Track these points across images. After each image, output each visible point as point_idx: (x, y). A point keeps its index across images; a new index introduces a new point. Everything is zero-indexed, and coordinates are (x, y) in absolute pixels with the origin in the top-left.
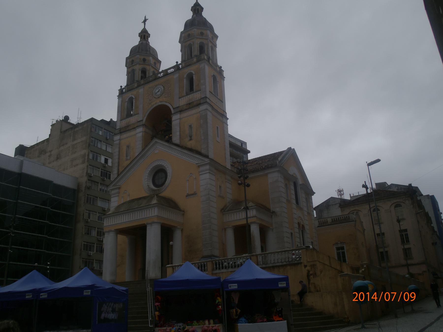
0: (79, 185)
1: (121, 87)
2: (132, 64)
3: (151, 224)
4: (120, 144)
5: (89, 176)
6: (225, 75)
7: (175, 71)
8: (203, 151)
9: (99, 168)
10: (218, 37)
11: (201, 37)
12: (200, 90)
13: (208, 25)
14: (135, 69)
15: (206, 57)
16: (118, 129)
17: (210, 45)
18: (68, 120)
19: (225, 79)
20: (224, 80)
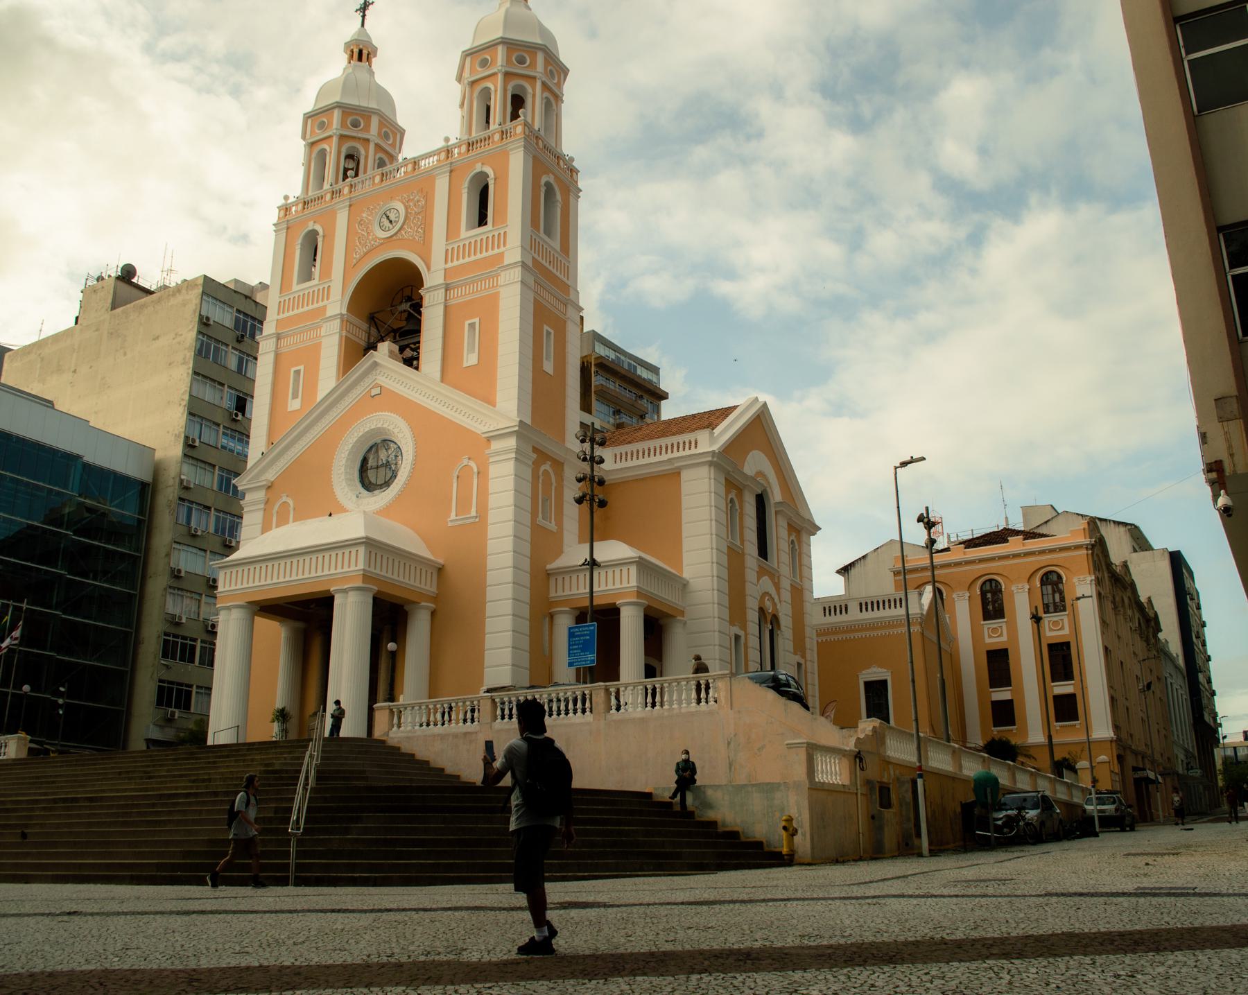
0: (157, 470)
1: (286, 198)
3: (345, 591)
9: (218, 425)
10: (568, 70)
18: (133, 278)
19: (580, 194)
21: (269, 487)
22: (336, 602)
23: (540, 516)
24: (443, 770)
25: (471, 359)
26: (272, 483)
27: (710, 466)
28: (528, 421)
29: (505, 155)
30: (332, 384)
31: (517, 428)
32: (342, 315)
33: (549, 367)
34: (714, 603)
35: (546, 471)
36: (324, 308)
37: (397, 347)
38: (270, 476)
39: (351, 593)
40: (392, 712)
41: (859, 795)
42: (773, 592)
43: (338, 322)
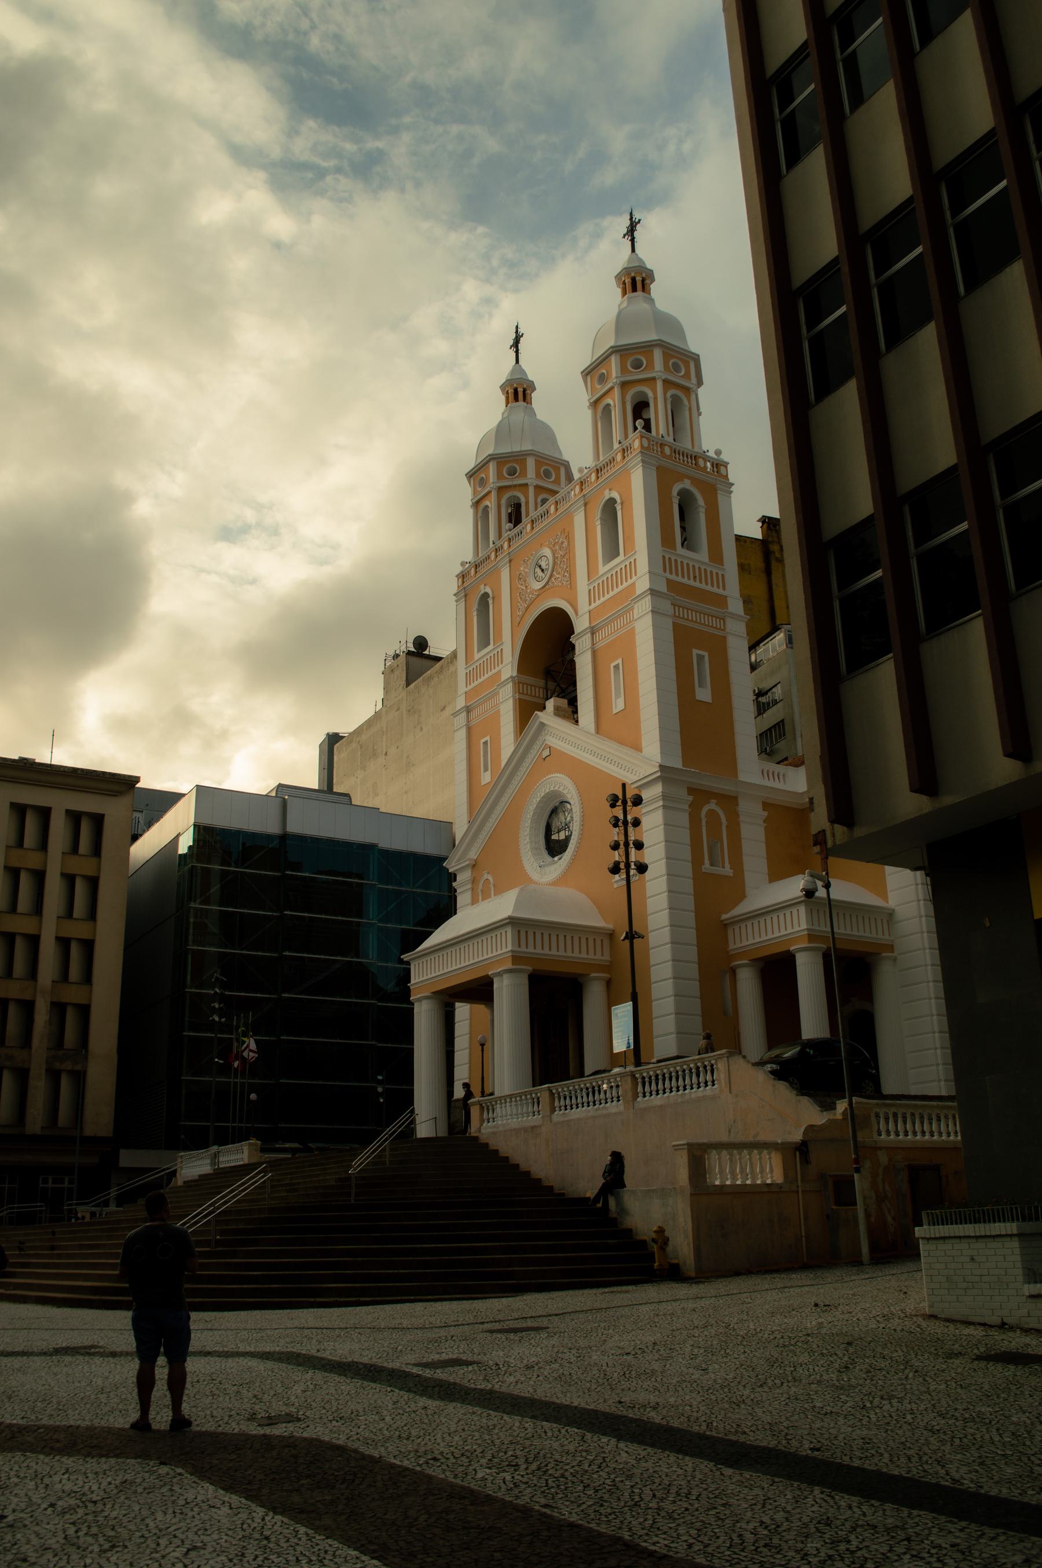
6: (732, 478)
19: (733, 488)
20: (732, 492)
21: (474, 865)
22: (495, 986)
23: (707, 861)
24: (518, 1165)
25: (618, 705)
26: (476, 860)
28: (678, 764)
29: (626, 473)
30: (511, 748)
32: (511, 677)
33: (704, 694)
34: (922, 932)
35: (711, 813)
36: (499, 673)
37: (566, 701)
38: (473, 855)
39: (505, 976)
40: (482, 1108)
41: (800, 1193)
43: (510, 686)
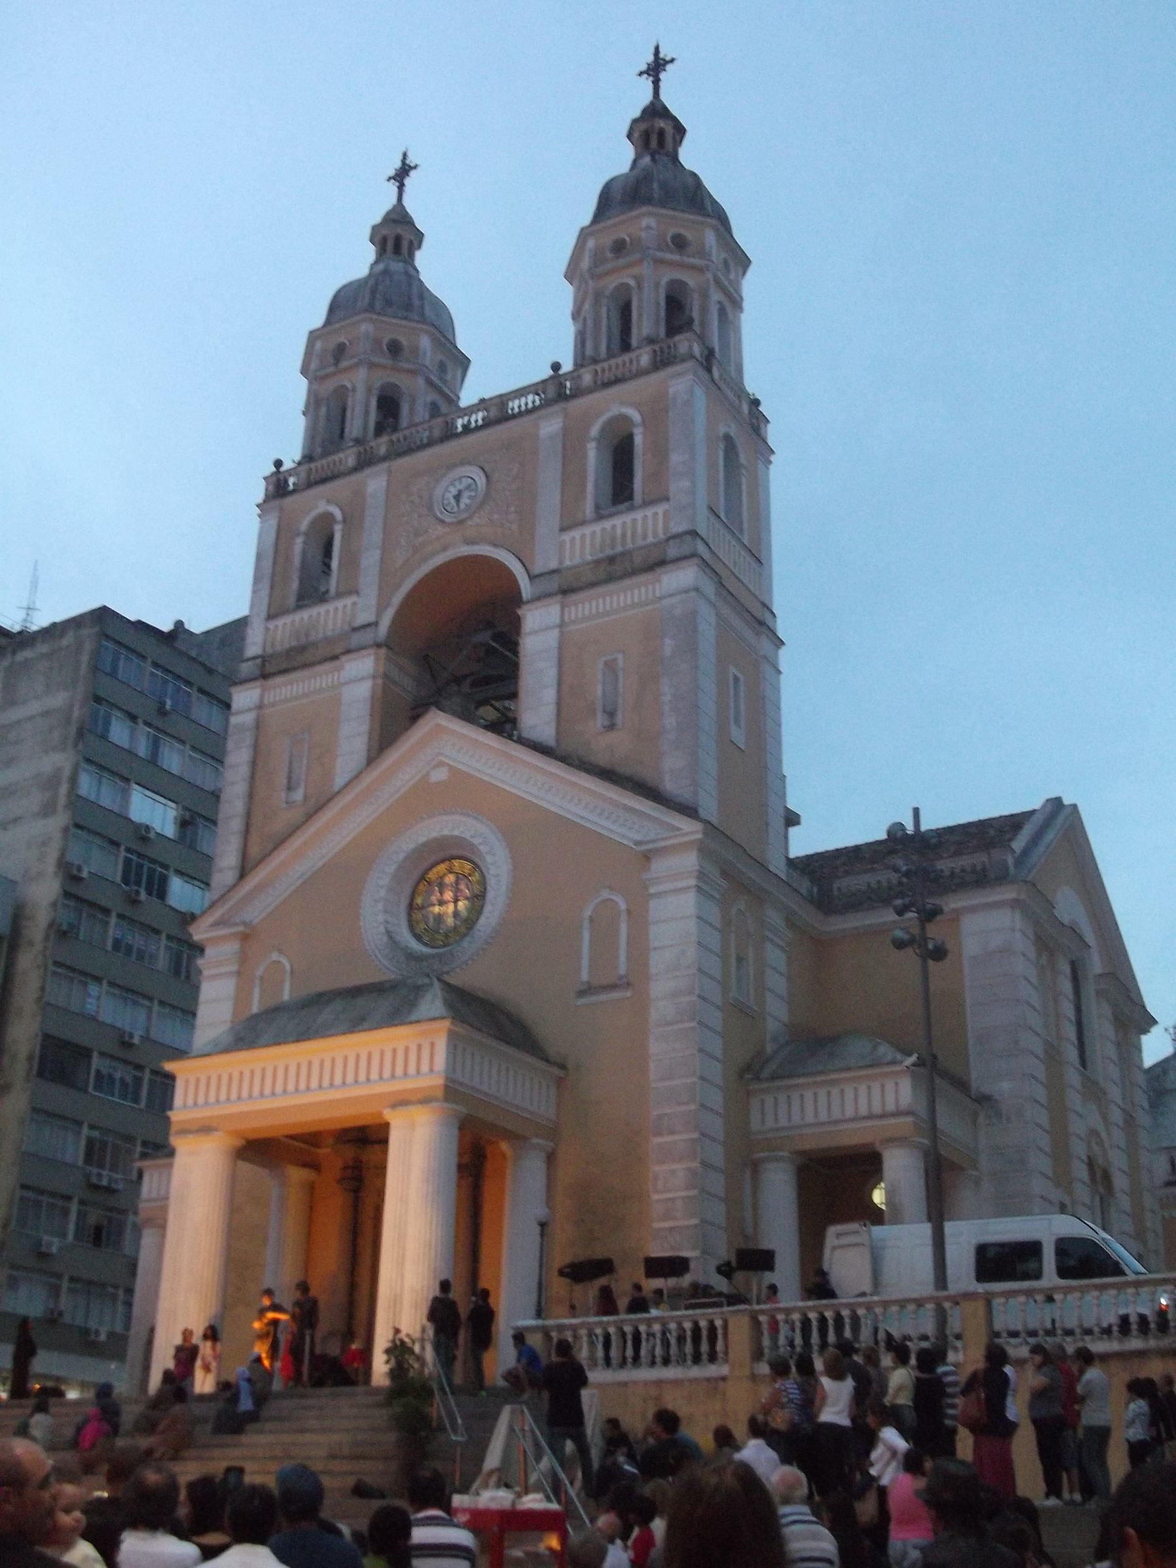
1: (278, 464)
2: (336, 364)
4: (258, 725)
5: (71, 876)
7: (546, 404)
8: (669, 786)
9: (116, 844)
11: (676, 257)
12: (667, 499)
13: (709, 208)
14: (349, 385)
15: (697, 350)
16: (254, 658)
17: (716, 296)
27: (1012, 907)
31: (699, 836)
42: (1100, 1127)
